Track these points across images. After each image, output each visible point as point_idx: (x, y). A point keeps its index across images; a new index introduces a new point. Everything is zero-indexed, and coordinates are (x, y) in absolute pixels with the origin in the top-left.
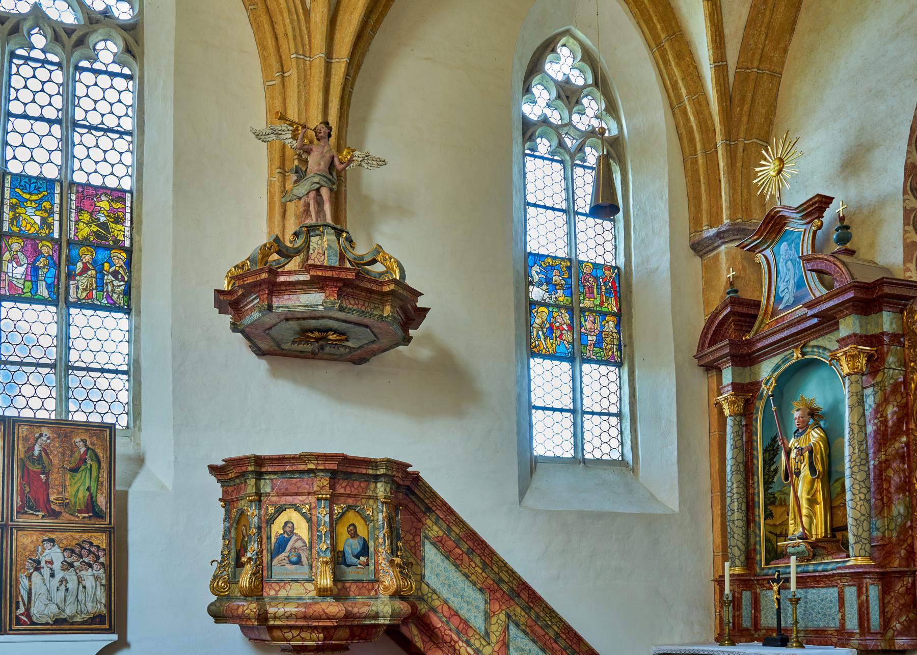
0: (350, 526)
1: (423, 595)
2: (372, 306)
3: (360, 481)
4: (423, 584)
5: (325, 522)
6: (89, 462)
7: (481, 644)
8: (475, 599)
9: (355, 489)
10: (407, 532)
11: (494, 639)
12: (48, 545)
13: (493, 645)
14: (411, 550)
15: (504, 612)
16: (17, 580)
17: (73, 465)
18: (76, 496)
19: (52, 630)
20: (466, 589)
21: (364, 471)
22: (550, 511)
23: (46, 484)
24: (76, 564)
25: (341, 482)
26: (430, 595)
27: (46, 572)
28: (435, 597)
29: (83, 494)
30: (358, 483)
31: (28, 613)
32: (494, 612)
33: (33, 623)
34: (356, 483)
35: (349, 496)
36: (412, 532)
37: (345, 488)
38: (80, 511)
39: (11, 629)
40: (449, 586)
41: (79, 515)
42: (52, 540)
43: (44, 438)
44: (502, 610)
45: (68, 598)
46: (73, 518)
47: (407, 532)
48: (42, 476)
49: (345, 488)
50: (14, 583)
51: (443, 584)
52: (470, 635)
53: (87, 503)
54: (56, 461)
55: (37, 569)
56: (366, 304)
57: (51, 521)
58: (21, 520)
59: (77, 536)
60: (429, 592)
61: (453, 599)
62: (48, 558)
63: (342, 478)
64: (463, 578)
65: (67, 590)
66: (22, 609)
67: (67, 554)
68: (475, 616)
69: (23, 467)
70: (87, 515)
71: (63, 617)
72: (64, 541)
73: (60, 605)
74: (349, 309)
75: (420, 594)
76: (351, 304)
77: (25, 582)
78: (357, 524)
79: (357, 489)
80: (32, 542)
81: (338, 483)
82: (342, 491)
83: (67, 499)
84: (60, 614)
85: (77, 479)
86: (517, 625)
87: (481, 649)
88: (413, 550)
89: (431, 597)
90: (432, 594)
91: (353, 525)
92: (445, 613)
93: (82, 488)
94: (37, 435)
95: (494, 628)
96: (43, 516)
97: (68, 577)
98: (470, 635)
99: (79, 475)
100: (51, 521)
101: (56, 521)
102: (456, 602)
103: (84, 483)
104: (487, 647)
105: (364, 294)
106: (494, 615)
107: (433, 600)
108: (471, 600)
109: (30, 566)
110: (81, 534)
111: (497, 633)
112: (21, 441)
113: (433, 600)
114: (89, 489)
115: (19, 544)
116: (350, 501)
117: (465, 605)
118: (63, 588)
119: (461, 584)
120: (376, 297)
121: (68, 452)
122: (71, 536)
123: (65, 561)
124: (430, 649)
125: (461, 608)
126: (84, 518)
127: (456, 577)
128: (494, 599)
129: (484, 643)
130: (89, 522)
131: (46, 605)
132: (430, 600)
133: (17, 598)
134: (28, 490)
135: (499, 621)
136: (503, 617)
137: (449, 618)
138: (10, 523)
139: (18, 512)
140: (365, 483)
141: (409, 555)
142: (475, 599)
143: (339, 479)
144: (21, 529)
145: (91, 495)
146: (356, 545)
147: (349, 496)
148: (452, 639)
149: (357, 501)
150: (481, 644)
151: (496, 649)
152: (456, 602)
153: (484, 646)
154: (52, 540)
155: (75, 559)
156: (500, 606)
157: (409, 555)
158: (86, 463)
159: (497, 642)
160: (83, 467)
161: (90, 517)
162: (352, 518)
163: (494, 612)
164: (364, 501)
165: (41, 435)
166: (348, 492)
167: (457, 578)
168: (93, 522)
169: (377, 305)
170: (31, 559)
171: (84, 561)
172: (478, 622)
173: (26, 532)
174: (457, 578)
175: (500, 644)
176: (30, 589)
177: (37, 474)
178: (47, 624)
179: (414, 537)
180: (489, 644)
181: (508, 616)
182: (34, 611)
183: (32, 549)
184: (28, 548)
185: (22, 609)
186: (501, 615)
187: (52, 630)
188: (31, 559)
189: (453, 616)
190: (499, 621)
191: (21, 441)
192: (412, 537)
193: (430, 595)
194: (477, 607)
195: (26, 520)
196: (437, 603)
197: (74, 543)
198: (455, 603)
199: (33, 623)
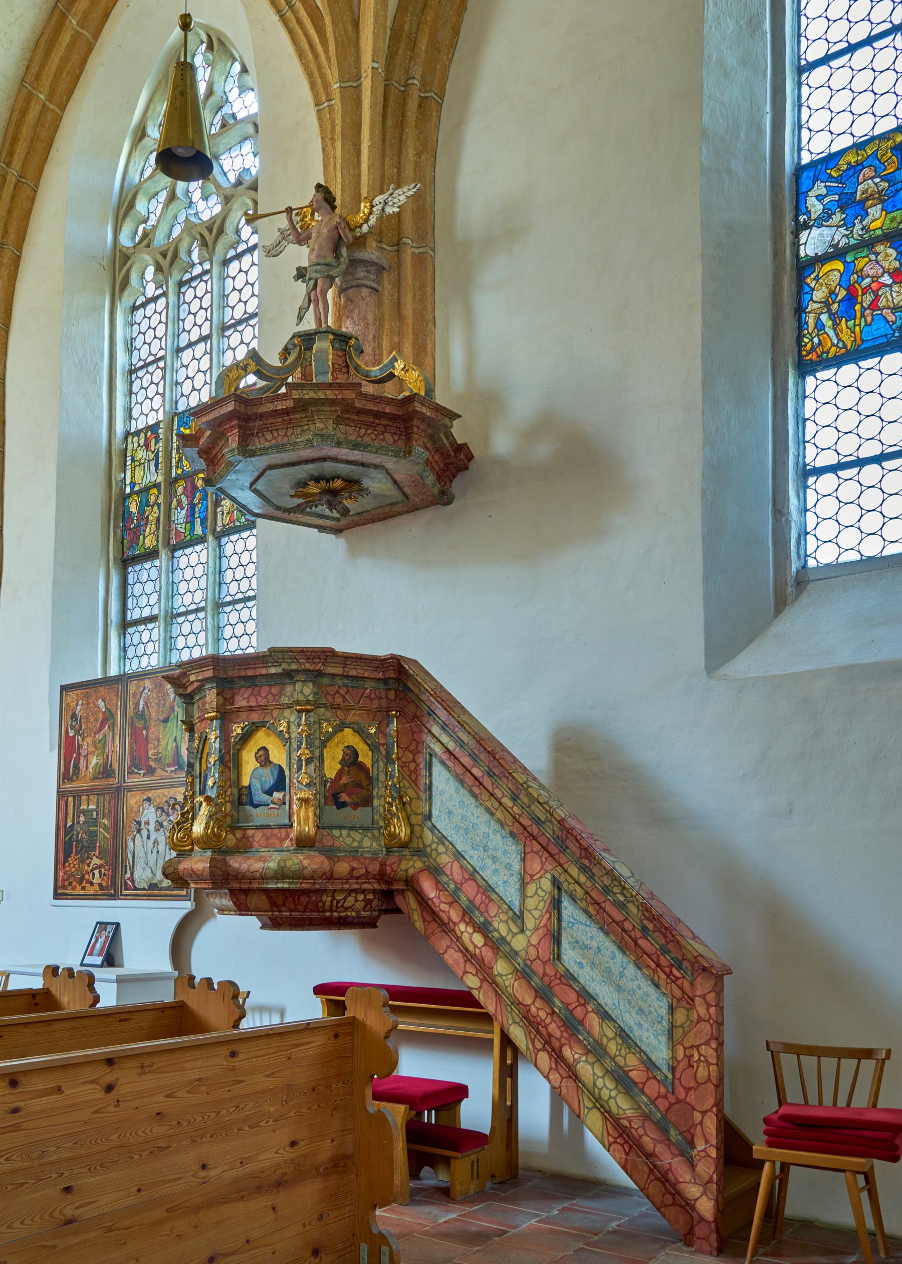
0: (259, 750)
1: (425, 846)
2: (298, 430)
3: (270, 686)
4: (425, 828)
5: (215, 749)
6: (176, 709)
7: (510, 930)
8: (505, 852)
9: (263, 698)
10: (406, 749)
11: (530, 923)
12: (146, 805)
13: (528, 933)
14: (410, 776)
15: (549, 876)
16: (126, 843)
17: (164, 716)
18: (166, 748)
19: (130, 895)
20: (491, 835)
21: (264, 671)
22: (772, 677)
23: (147, 739)
24: (165, 823)
25: (242, 690)
26: (434, 846)
27: (144, 833)
28: (441, 849)
29: (171, 745)
30: (267, 689)
31: (132, 879)
32: (532, 876)
33: (136, 889)
34: (264, 691)
35: (250, 709)
36: (412, 748)
37: (248, 699)
38: (169, 766)
39: (122, 895)
40: (466, 831)
41: (168, 769)
42: (149, 800)
43: (146, 691)
44: (546, 872)
45: (159, 861)
46: (164, 773)
47: (406, 749)
48: (144, 732)
49: (248, 699)
50: (124, 846)
51: (457, 828)
52: (493, 914)
53: (174, 755)
54: (153, 714)
55: (139, 831)
56: (289, 433)
57: (149, 779)
58: (131, 781)
59: (166, 791)
60: (433, 842)
61: (471, 852)
62: (145, 819)
63: (243, 686)
64: (487, 816)
65: (158, 852)
66: (128, 875)
67: (159, 813)
68: (505, 882)
69: (133, 725)
70: (173, 769)
71: (155, 882)
72: (157, 800)
73: (153, 869)
74: (260, 449)
75: (421, 846)
76: (266, 440)
77: (130, 844)
78: (269, 747)
79: (266, 697)
80: (136, 802)
81: (238, 693)
82: (244, 703)
83: (160, 753)
84: (153, 878)
85: (167, 729)
86: (573, 898)
87: (509, 939)
88: (413, 777)
89: (436, 850)
90: (438, 844)
91: (265, 749)
92: (455, 874)
93: (170, 739)
94: (142, 689)
95: (531, 903)
96: (144, 774)
97: (159, 839)
98: (493, 914)
99: (169, 725)
100: (149, 779)
101: (152, 778)
102: (476, 857)
103: (172, 733)
104: (519, 936)
105: (280, 420)
106: (532, 880)
107: (438, 854)
108: (499, 854)
109: (134, 826)
110: (169, 790)
111: (537, 914)
112: (131, 698)
113: (438, 854)
114: (175, 740)
115: (128, 805)
116: (255, 717)
117: (489, 862)
118: (155, 851)
119: (484, 829)
120: (298, 416)
121: (162, 702)
122: (162, 793)
123: (157, 821)
124: (433, 933)
125: (484, 868)
126: (172, 771)
127: (476, 814)
128: (532, 851)
129: (515, 929)
130: (175, 776)
131: (144, 869)
132: (434, 854)
133: (126, 862)
134: (135, 748)
135: (540, 891)
136: (546, 884)
137: (462, 884)
138: (123, 785)
139: (128, 773)
140: (278, 687)
141: (407, 785)
142: (505, 852)
143: (239, 689)
144: (130, 789)
145: (177, 746)
146: (269, 778)
147: (250, 709)
148: (450, 919)
149: (266, 714)
150: (510, 930)
151: (534, 941)
152: (476, 857)
153: (514, 935)
154: (149, 800)
155: (165, 817)
156: (543, 865)
157: (407, 785)
158: (174, 710)
159: (536, 929)
160: (172, 716)
161: (176, 769)
162: (261, 739)
163: (532, 876)
164: (275, 713)
165: (144, 688)
166: (253, 703)
167: (478, 817)
168: (177, 776)
169: (306, 427)
170: (135, 821)
171: (170, 820)
172: (511, 894)
173: (133, 793)
174: (478, 817)
175: (541, 932)
176: (134, 853)
177: (141, 730)
178: (144, 889)
179: (414, 755)
180: (522, 931)
181: (556, 883)
182: (136, 875)
183: (136, 810)
184: (134, 810)
185: (128, 875)
186: (543, 880)
187: (130, 895)
188: (135, 821)
189: (466, 880)
190: (540, 891)
191: (131, 698)
192: (411, 756)
193: (434, 846)
194: (508, 867)
195: (135, 780)
196: (445, 859)
197: (163, 801)
198: (474, 857)
199: (136, 889)
